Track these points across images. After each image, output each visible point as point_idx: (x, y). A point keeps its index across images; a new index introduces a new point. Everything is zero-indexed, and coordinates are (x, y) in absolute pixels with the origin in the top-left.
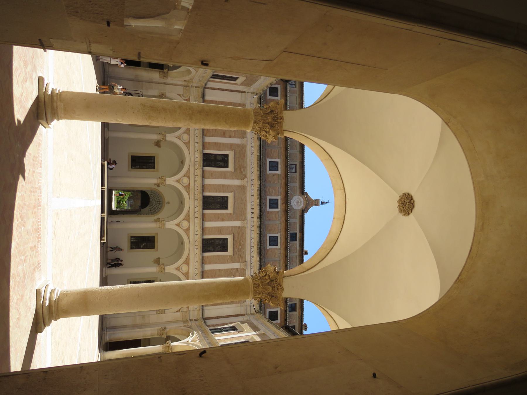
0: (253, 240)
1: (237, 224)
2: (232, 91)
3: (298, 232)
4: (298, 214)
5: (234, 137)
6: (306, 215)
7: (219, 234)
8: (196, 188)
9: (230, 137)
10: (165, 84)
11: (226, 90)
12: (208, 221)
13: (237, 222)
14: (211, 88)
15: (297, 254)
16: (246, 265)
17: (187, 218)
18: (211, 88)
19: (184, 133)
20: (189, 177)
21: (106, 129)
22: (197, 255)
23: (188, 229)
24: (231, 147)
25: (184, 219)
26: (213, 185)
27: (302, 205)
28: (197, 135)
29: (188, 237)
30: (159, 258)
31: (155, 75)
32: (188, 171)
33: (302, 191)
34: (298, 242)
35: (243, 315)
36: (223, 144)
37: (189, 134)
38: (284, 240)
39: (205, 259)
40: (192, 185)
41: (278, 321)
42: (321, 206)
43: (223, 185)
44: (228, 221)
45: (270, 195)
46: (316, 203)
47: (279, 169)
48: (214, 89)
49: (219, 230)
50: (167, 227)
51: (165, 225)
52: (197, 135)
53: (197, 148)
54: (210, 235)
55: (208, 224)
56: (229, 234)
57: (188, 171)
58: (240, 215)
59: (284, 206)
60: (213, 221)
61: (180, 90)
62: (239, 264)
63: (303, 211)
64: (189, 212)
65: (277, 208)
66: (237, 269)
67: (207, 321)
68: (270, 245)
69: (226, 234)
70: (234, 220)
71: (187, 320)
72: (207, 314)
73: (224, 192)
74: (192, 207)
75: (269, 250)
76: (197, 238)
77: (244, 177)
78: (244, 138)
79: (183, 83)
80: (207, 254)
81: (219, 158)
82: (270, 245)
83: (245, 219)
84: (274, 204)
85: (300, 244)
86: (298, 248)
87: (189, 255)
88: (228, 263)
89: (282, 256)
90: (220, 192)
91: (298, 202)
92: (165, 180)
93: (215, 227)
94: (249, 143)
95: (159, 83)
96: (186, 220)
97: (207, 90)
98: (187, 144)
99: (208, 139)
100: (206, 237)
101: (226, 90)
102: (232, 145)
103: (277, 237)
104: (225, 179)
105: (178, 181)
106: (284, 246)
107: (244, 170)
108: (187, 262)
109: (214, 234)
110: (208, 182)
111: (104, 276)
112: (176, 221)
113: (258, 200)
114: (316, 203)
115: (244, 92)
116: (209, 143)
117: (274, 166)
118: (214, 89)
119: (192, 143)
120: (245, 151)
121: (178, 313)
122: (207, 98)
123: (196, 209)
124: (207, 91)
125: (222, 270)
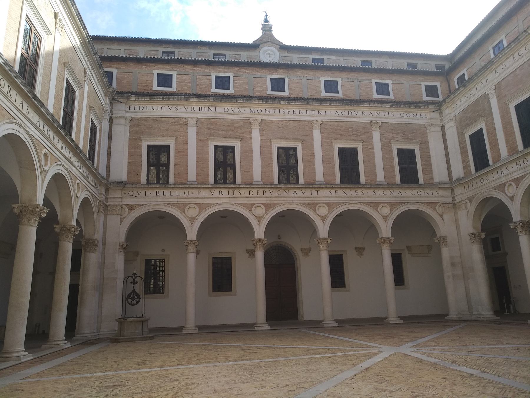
0: (340, 112)
1: (317, 134)
2: (110, 140)
3: (311, 57)
4: (285, 54)
5: (186, 136)
6: (287, 42)
7: (333, 160)
8: (268, 194)
9: (186, 142)
10: (104, 244)
11: (109, 147)
12: (315, 176)
13: (314, 135)
14: (108, 171)
15: (342, 59)
16: (376, 123)
17: (313, 206)
18: (108, 171)
19: (184, 212)
20: (253, 204)
21: (184, 332)
22: (365, 191)
23: (329, 205)
24: (201, 142)
25: (315, 211)
26: (262, 169)
27: (273, 48)
28: (187, 193)
29: (339, 204)
30: (356, 248)
31: (92, 259)
32: (244, 205)
33: (255, 46)
34: (325, 57)
35: (443, 127)
36: (197, 153)
37: (185, 205)
38: (329, 73)
39: (369, 181)
40: (264, 200)
41: (438, 84)
42: (271, 22)
43: (262, 154)
44: (313, 147)
45: (267, 90)
46: (267, 28)
47: (227, 75)
48: (108, 166)
49: (327, 161)
50: (327, 237)
51: (321, 239)
52: (187, 193)
53: (207, 192)
54: (334, 174)
55: (320, 177)
56: (332, 146)
57: (244, 205)
58: (304, 129)
59: (281, 71)
60: (314, 169)
61: (113, 220)
62: (374, 133)
63: (283, 48)
64: (304, 204)
65: (283, 80)
66: (381, 135)
67: (454, 177)
68: (338, 93)
69: (332, 150)
70: (312, 139)
71: (454, 204)
72: (445, 178)
73: (271, 154)
74: (297, 200)
75: (344, 95)
76: (340, 192)
77: (248, 123)
78: (186, 122)
79: (102, 216)
80: (363, 180)
81: (221, 158)
82: (338, 93)
83: (311, 123)
84: (277, 84)
85: (327, 55)
86: (334, 57)
87: (365, 203)
88: (373, 148)
89: (352, 76)
90: (271, 159)
91: (269, 54)
92: (260, 239)
93: (324, 167)
94: (194, 115)
95: (104, 253)
96: (315, 207)
97: (112, 177)
98: (201, 207)
99: (192, 176)
100: (338, 180)
101: (109, 147)
102: (198, 140)
103: (325, 82)
104: (251, 151)
105: (259, 219)
106: (338, 73)
107: (237, 123)
108: (375, 206)
109: (334, 168)
110: (257, 177)
111: (402, 322)
112: (318, 222)
113: (282, 102)
114: (267, 28)
115: (111, 119)
116: (197, 174)
117: (222, 82)
118: (108, 166)
119: (199, 201)
120: (207, 120)
121: (446, 217)
122: (124, 177)
123: (299, 193)
124: (112, 177)
125: (383, 156)
